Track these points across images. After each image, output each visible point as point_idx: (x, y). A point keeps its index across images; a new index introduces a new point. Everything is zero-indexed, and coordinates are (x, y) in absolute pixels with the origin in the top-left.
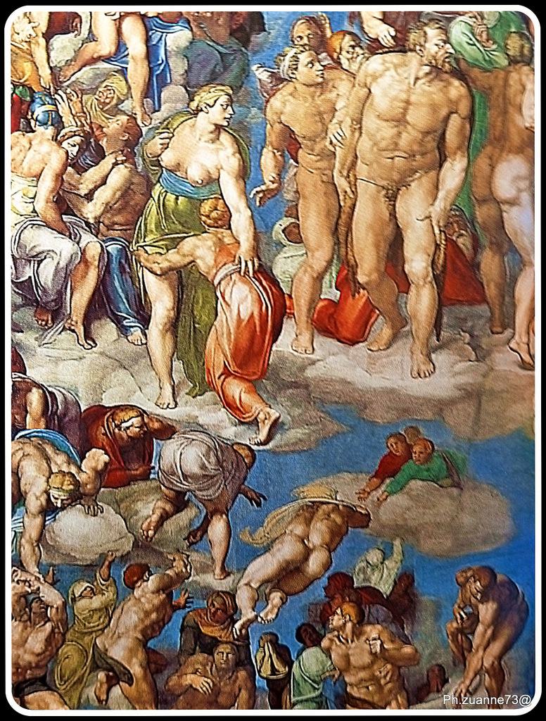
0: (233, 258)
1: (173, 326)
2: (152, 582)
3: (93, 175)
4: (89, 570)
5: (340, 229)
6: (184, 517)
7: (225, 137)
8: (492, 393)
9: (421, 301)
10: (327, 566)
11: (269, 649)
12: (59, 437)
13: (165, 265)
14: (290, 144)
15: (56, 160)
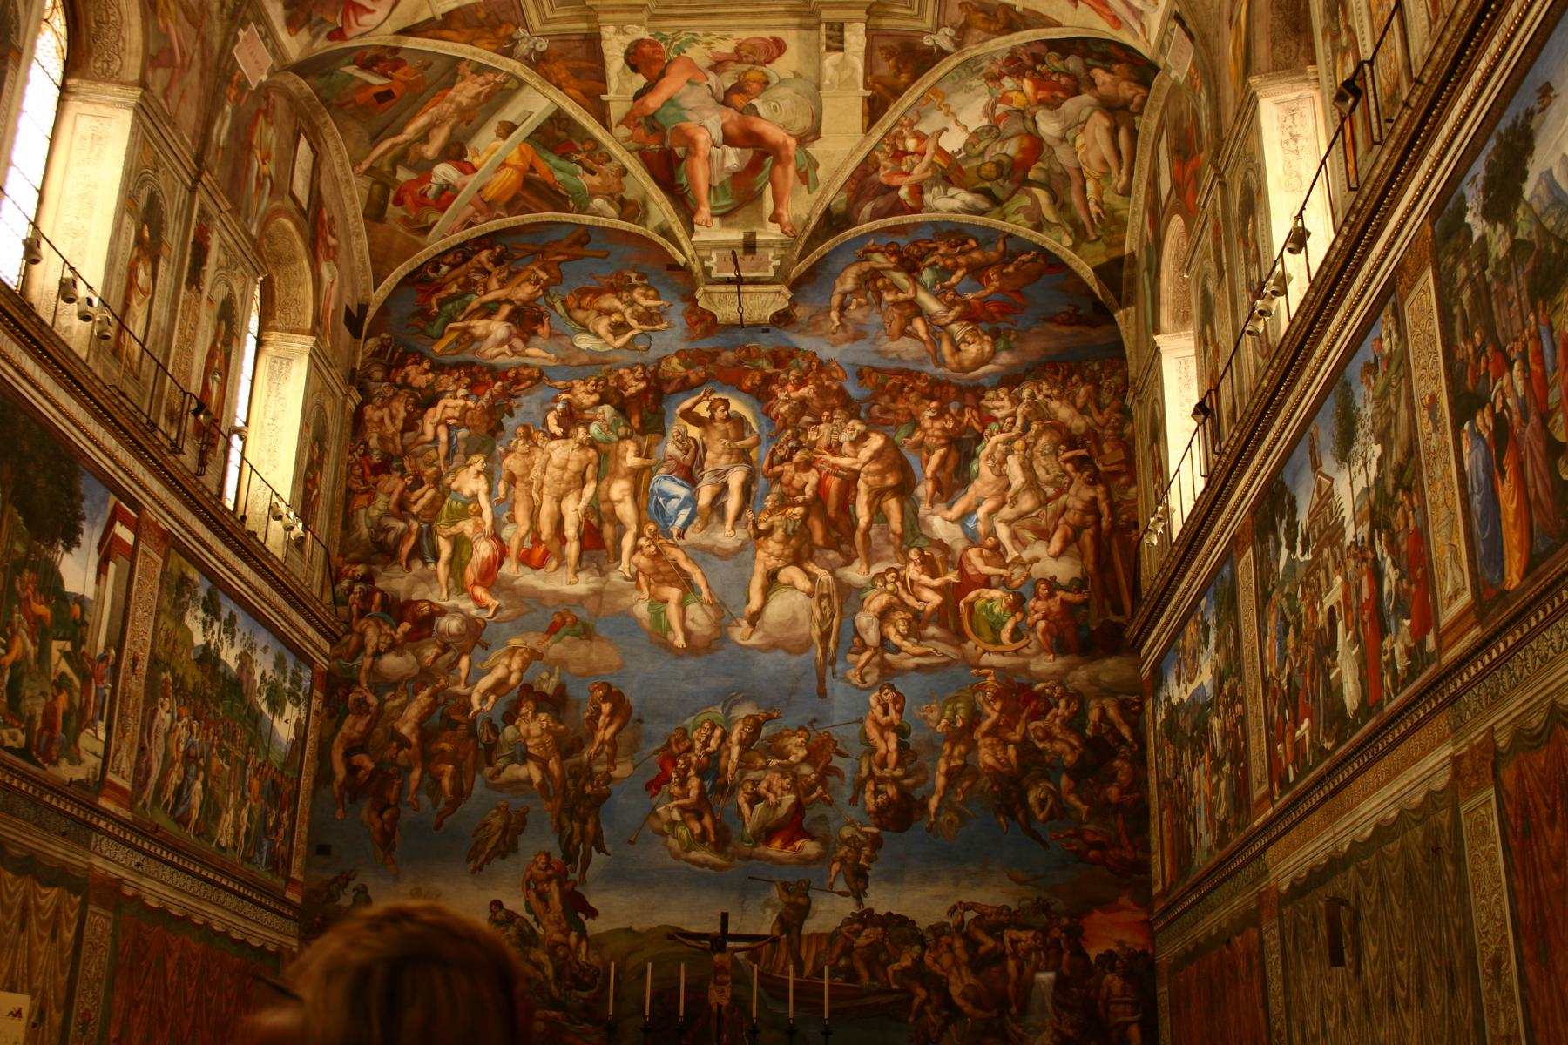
0: (482, 530)
1: (450, 562)
2: (427, 692)
3: (418, 493)
4: (394, 684)
5: (534, 516)
6: (448, 656)
7: (482, 477)
8: (609, 593)
9: (572, 549)
10: (520, 679)
11: (487, 727)
12: (388, 617)
13: (448, 533)
14: (512, 479)
15: (400, 487)
